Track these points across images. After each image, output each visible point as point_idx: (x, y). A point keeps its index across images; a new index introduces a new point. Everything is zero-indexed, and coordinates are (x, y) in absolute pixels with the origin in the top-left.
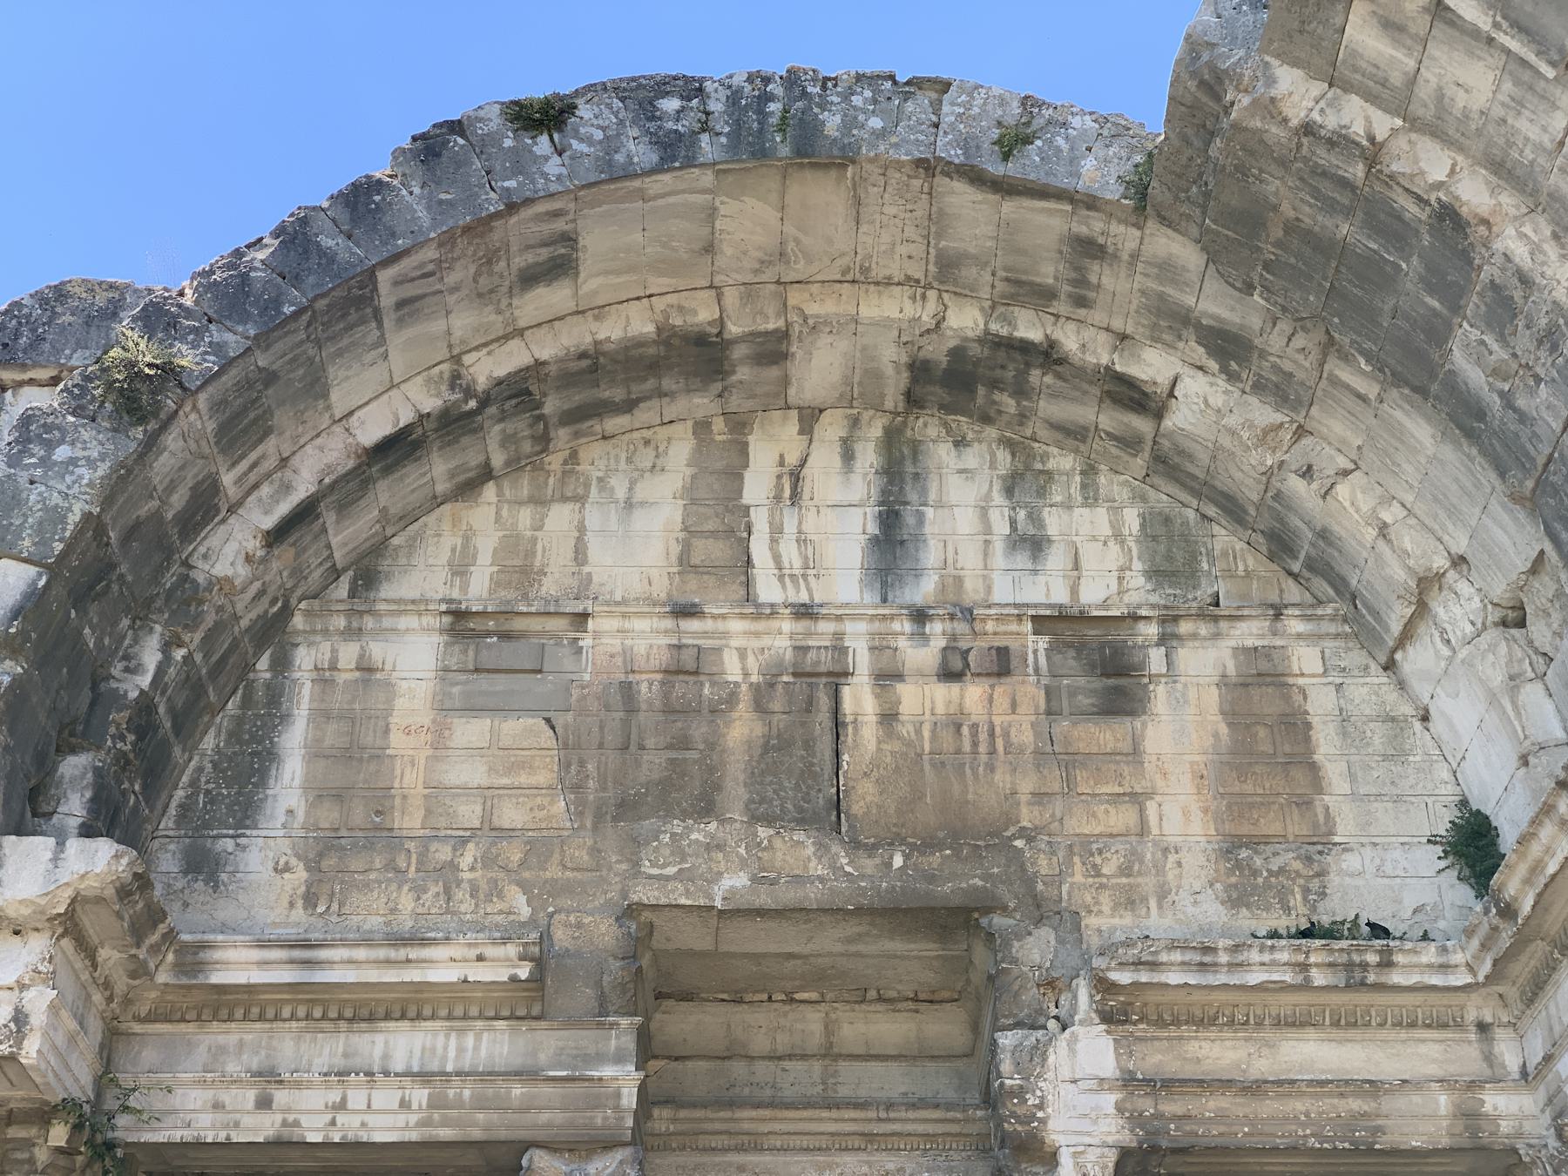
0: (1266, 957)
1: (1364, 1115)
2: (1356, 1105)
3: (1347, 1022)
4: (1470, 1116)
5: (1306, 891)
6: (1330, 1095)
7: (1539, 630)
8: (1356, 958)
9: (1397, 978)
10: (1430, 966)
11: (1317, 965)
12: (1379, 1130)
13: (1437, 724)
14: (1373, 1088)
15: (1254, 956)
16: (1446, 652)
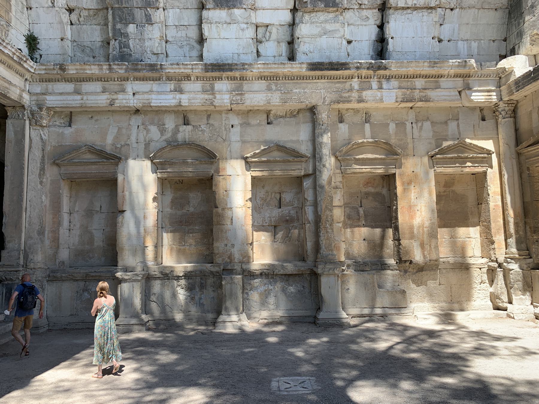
0: (11, 49)
1: (7, 88)
2: (6, 85)
3: (9, 67)
4: (21, 96)
5: (5, 33)
6: (4, 81)
7: (74, 17)
8: (23, 58)
9: (25, 65)
10: (30, 66)
11: (16, 55)
12: (8, 92)
13: (33, 12)
14: (10, 83)
15: (9, 47)
16: (51, 4)
